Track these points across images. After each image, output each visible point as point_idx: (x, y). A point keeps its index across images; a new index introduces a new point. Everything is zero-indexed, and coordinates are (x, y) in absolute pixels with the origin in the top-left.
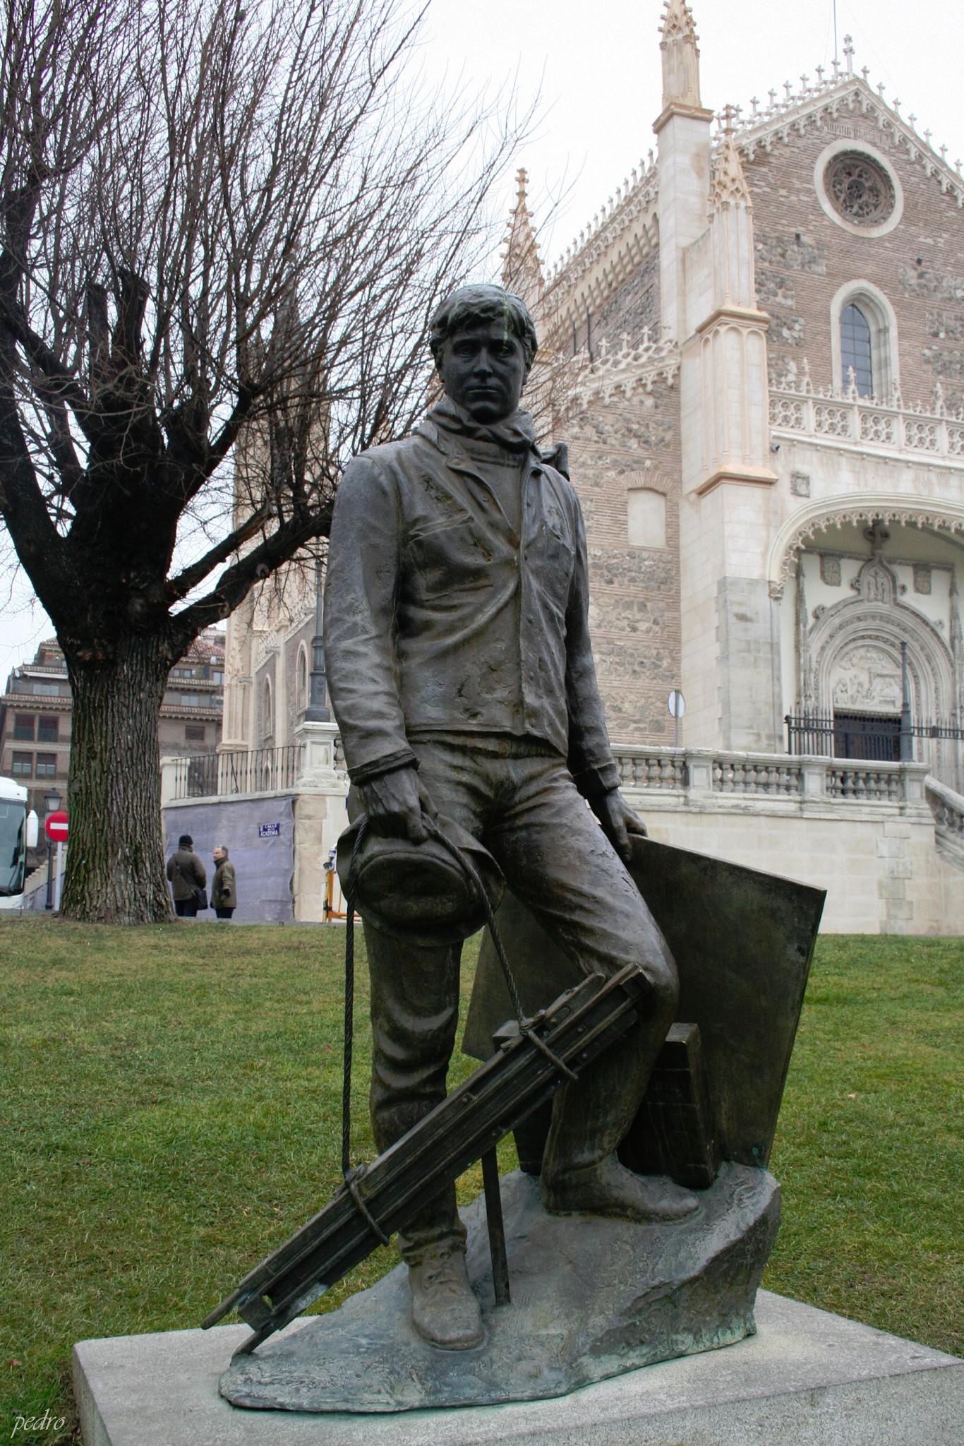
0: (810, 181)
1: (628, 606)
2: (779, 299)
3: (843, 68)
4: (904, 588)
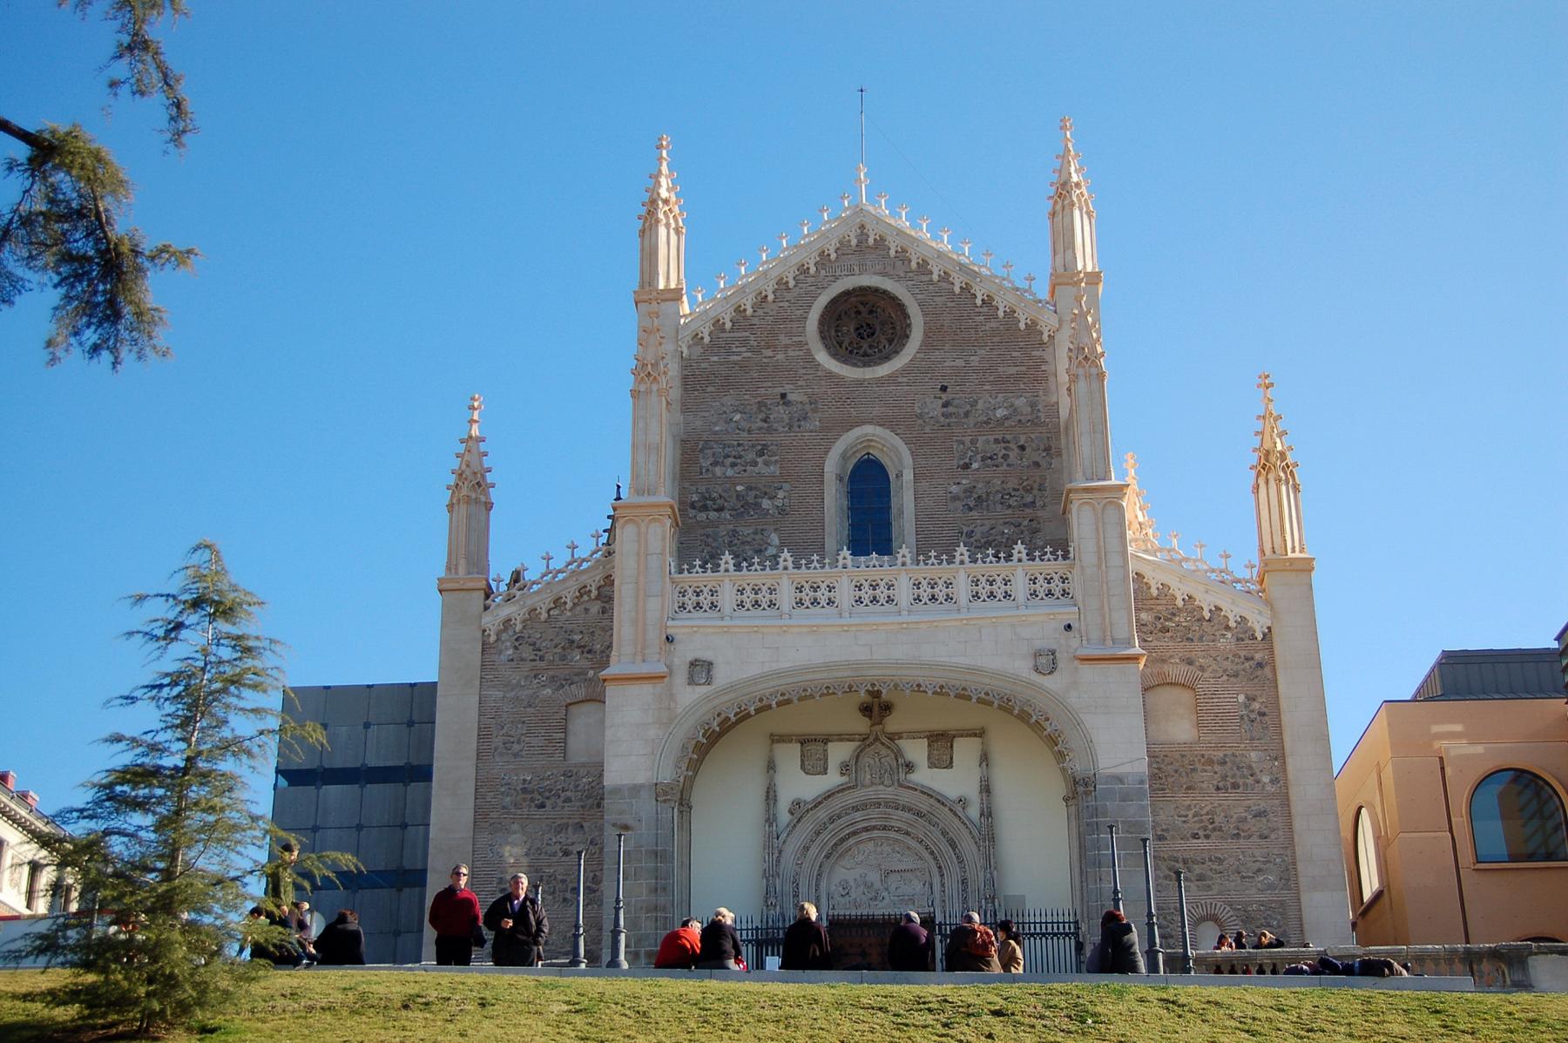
0: (803, 333)
1: (561, 829)
2: (761, 468)
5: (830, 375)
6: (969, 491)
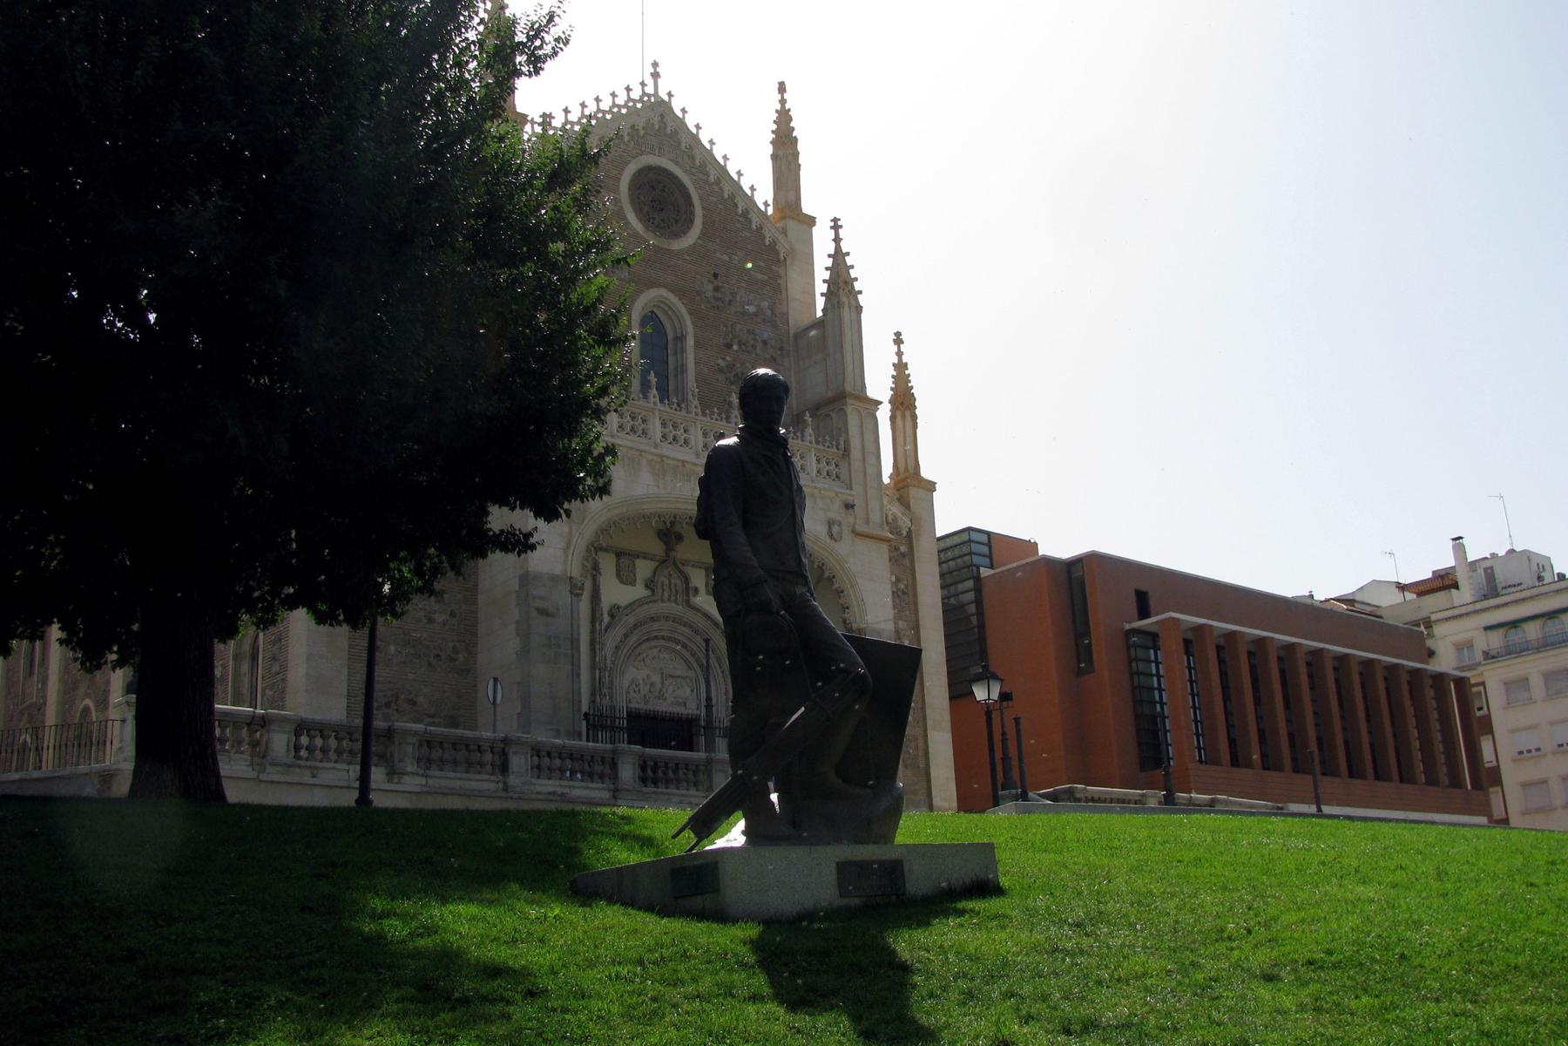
3: (650, 90)
4: (696, 590)
5: (636, 235)
6: (731, 366)
